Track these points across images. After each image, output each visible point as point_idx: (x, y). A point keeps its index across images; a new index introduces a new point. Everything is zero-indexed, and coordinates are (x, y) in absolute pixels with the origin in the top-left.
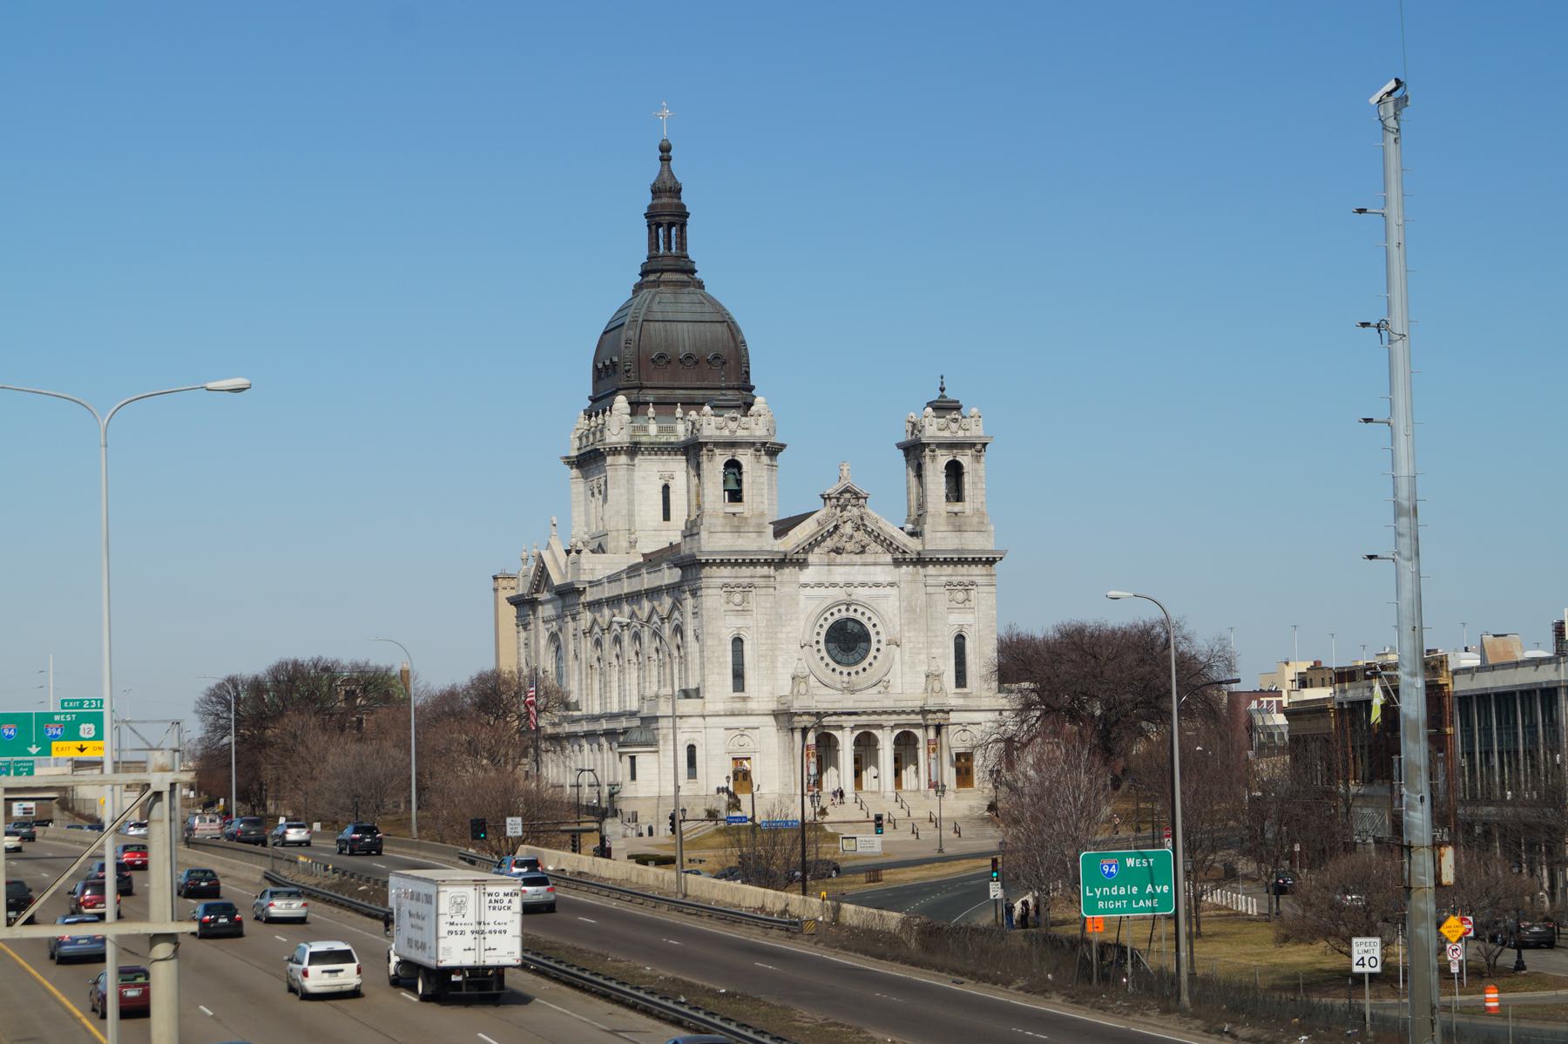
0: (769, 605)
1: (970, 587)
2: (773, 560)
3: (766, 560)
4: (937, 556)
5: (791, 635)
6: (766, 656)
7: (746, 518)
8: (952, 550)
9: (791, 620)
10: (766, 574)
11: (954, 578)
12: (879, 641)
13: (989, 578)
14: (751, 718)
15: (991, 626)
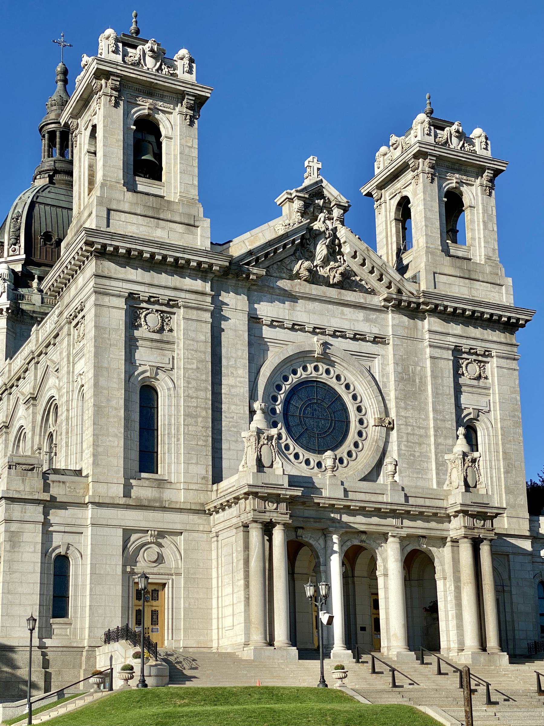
0: (203, 338)
1: (484, 359)
2: (211, 265)
3: (200, 263)
4: (446, 303)
5: (233, 391)
6: (196, 417)
7: (169, 202)
8: (464, 299)
9: (236, 368)
10: (200, 289)
11: (464, 341)
12: (361, 422)
13: (509, 348)
14: (169, 516)
15: (514, 416)
